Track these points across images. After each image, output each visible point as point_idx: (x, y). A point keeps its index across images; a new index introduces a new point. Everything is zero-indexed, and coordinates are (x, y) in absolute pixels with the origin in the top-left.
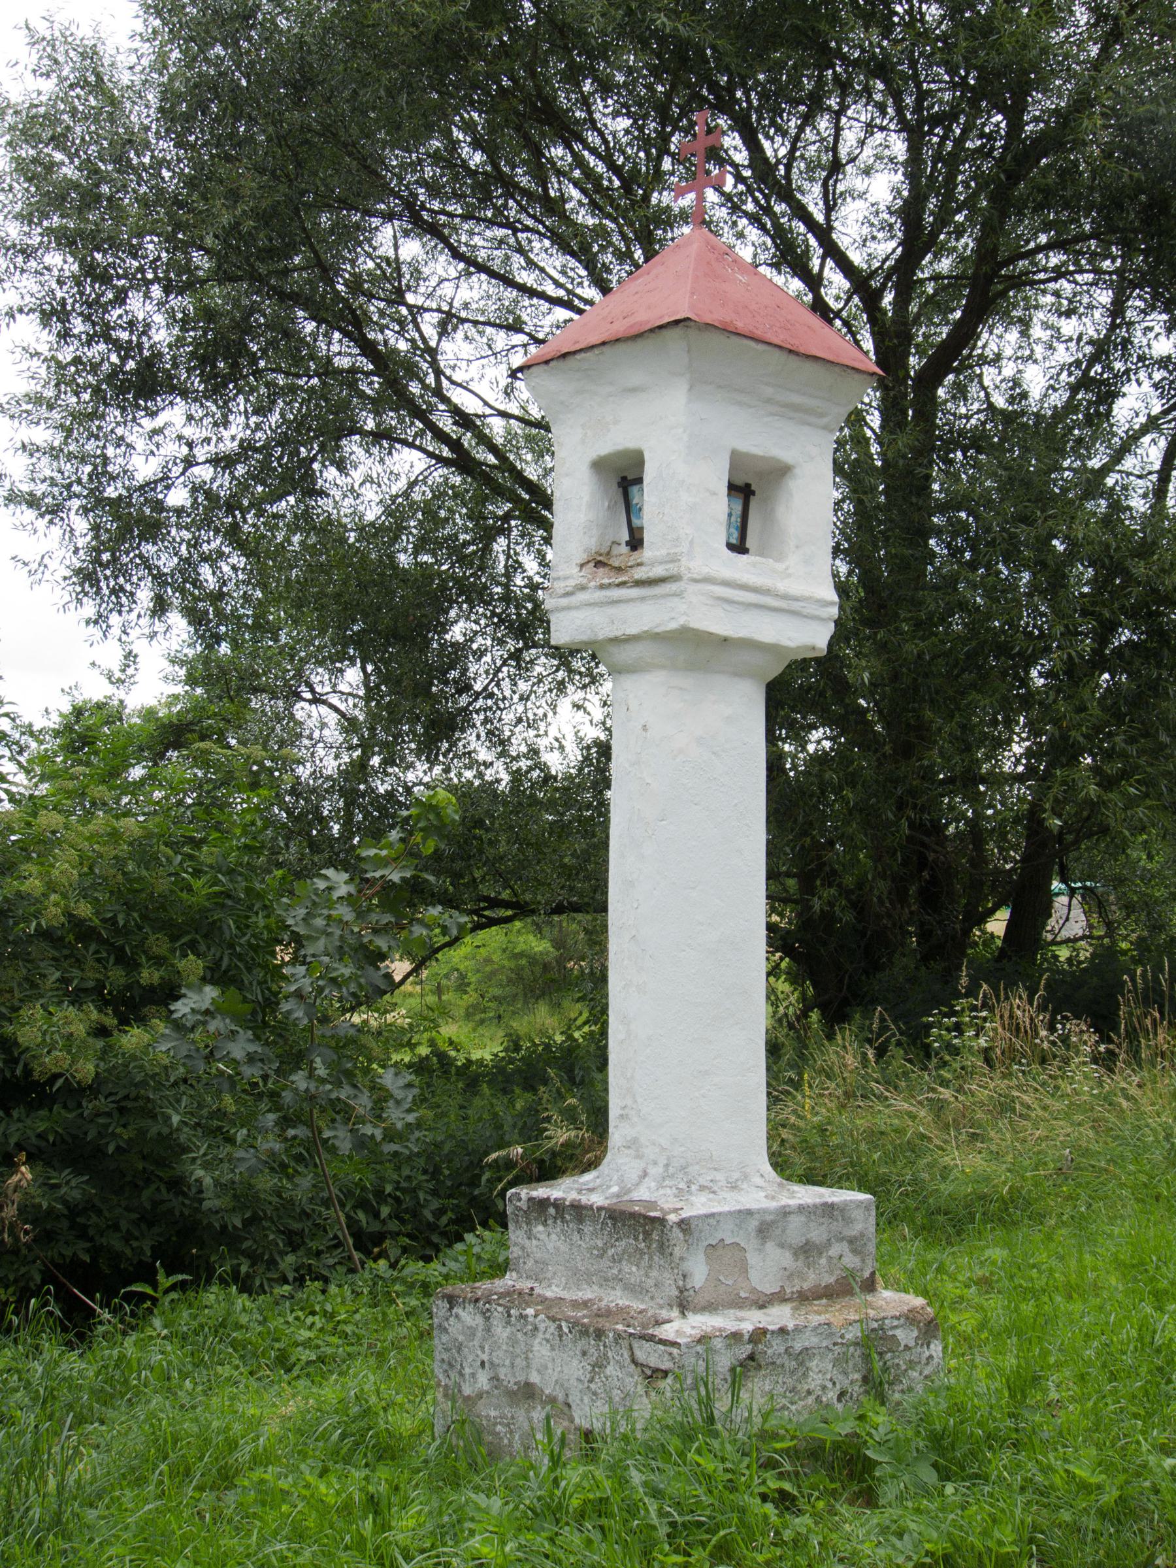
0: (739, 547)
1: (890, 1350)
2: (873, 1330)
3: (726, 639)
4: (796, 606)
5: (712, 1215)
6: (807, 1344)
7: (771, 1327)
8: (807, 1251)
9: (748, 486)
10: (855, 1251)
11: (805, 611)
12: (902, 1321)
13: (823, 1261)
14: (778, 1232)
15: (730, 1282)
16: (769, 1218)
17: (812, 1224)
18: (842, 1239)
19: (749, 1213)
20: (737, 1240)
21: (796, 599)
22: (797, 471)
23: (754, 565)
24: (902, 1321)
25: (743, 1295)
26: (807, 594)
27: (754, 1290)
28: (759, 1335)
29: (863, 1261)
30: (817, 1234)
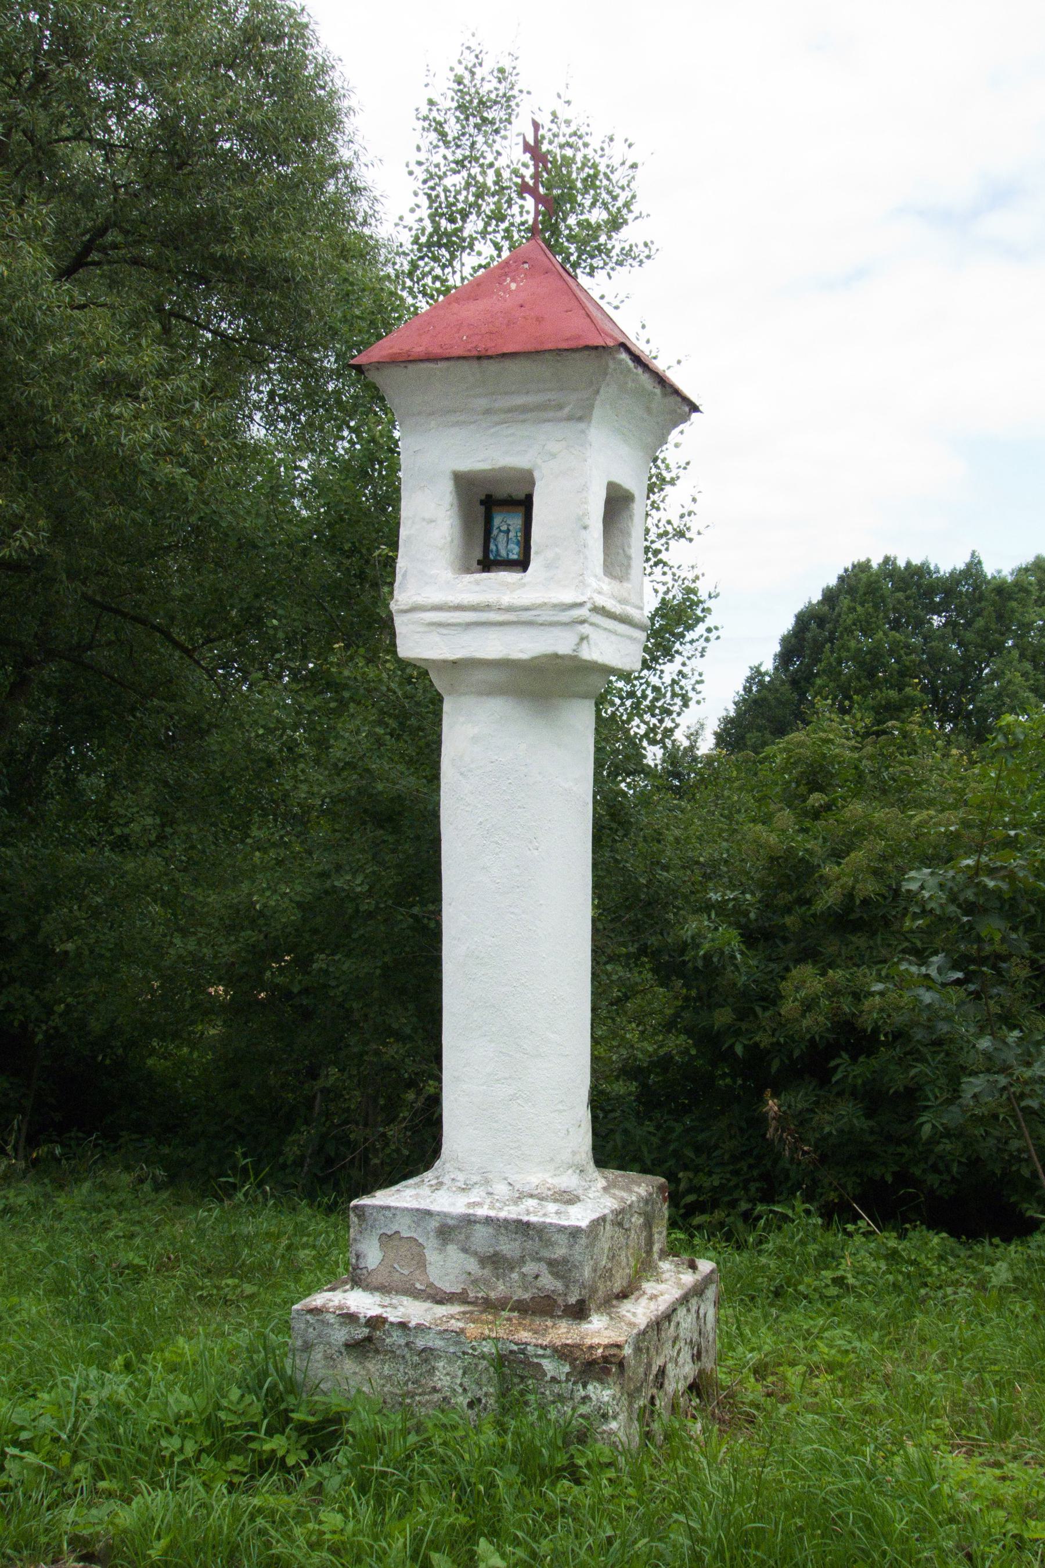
0: (488, 564)
1: (533, 1377)
2: (511, 1352)
3: (454, 663)
4: (526, 616)
5: (388, 1208)
6: (430, 1344)
7: (391, 1319)
8: (495, 1262)
9: (482, 502)
10: (556, 1275)
11: (540, 620)
12: (548, 1352)
13: (515, 1276)
14: (462, 1237)
15: (406, 1272)
16: (451, 1222)
17: (501, 1238)
18: (540, 1260)
19: (428, 1213)
20: (414, 1235)
21: (527, 609)
22: (536, 475)
23: (477, 583)
24: (548, 1352)
25: (418, 1286)
26: (539, 601)
27: (431, 1285)
28: (376, 1322)
29: (567, 1287)
30: (509, 1247)
